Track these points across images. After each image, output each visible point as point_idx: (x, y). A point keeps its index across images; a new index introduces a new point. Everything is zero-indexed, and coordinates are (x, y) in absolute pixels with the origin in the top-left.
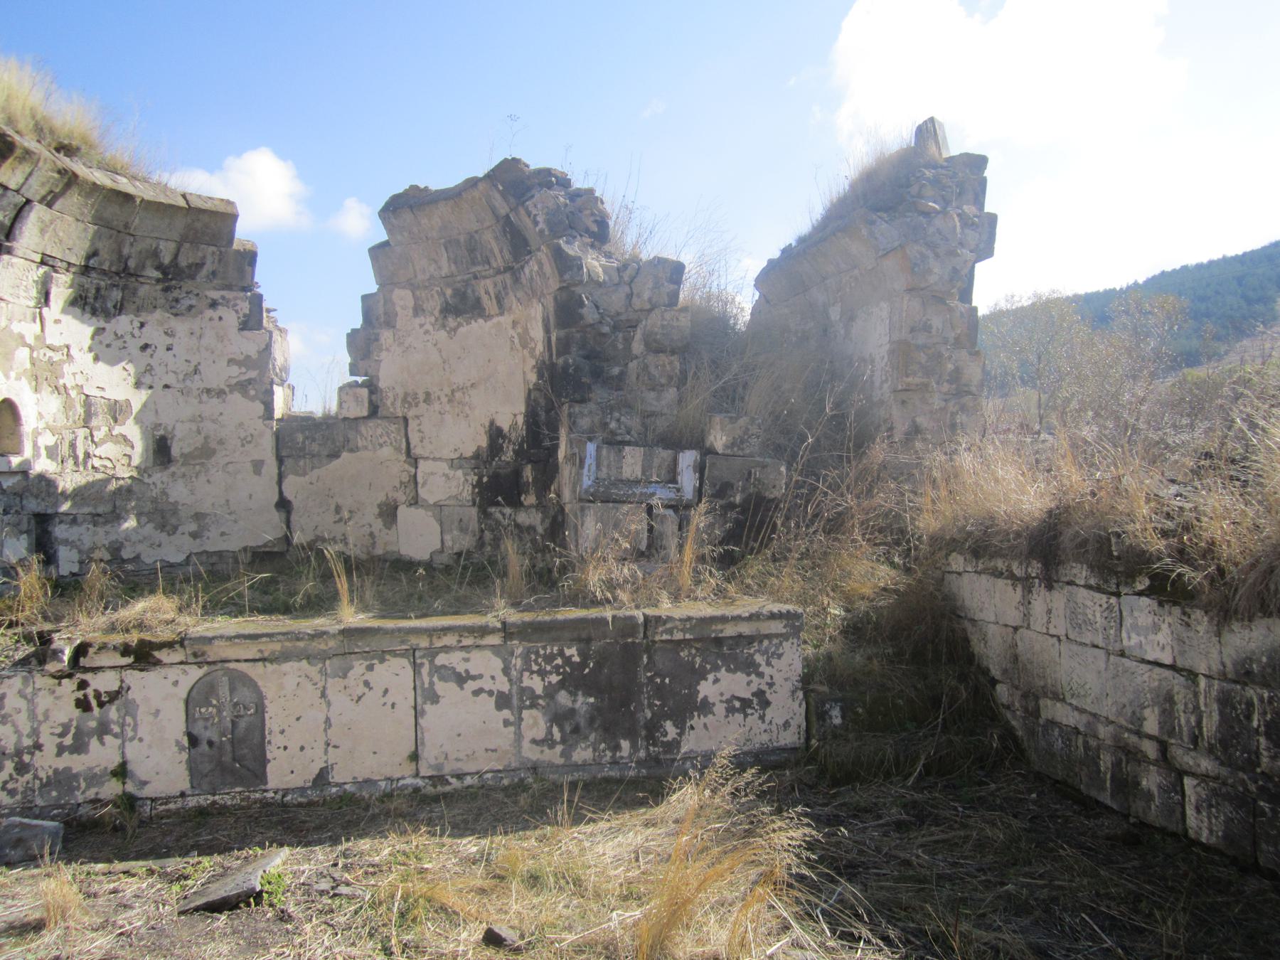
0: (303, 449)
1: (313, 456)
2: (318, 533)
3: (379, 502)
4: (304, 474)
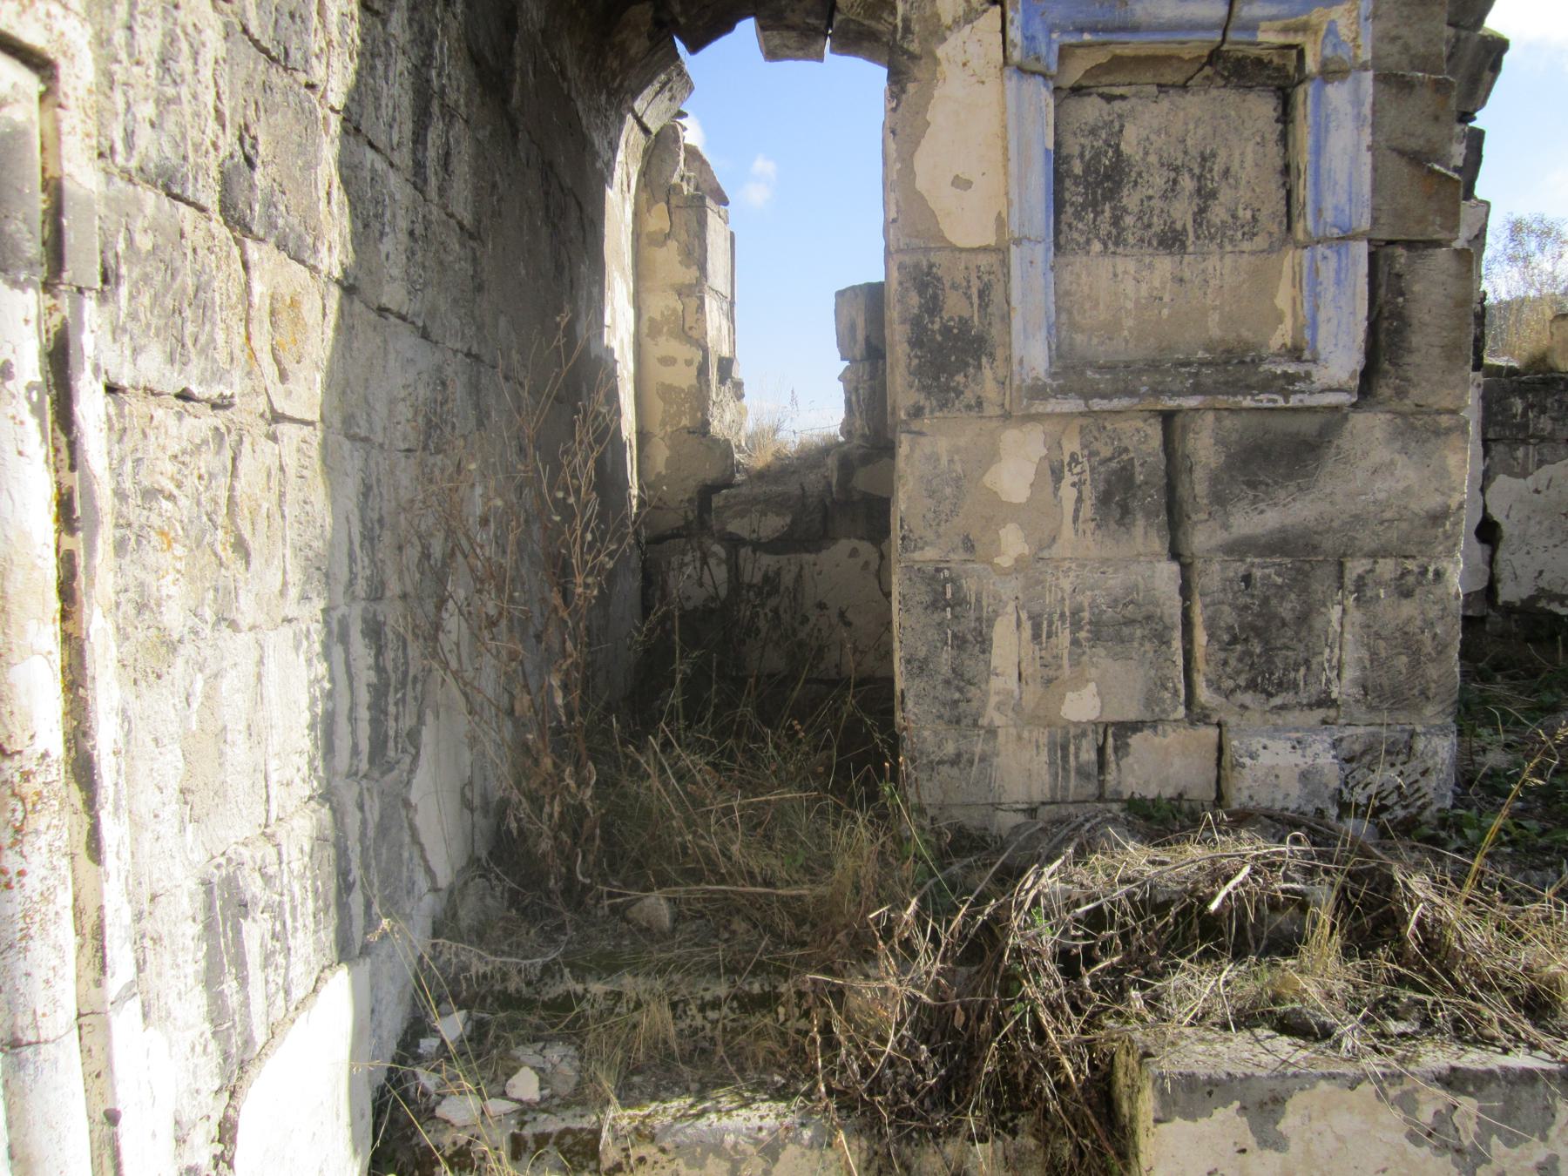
0: (1524, 426)
1: (1542, 439)
2: (1543, 583)
4: (1525, 474)
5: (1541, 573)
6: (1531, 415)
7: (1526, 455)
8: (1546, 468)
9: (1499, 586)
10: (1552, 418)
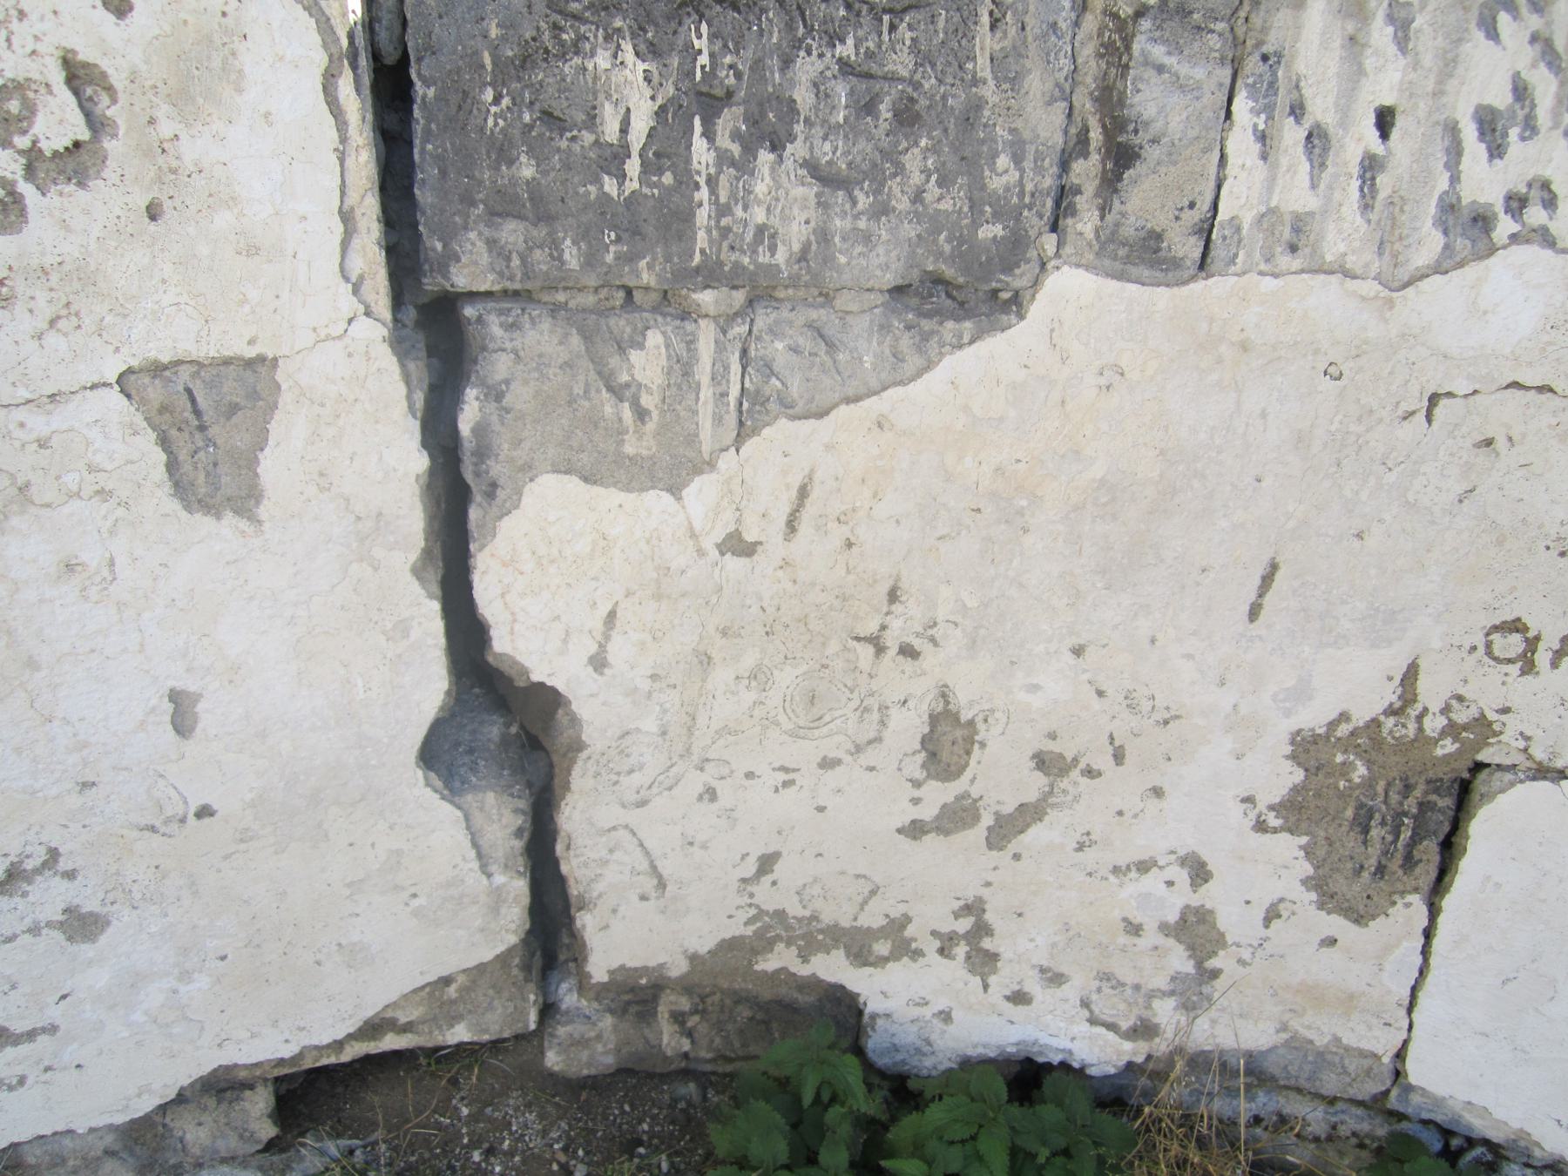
2: (767, 896)
3: (1313, 717)
5: (767, 863)
6: (701, 153)
7: (683, 367)
8: (779, 432)
9: (586, 922)
10: (814, 171)
